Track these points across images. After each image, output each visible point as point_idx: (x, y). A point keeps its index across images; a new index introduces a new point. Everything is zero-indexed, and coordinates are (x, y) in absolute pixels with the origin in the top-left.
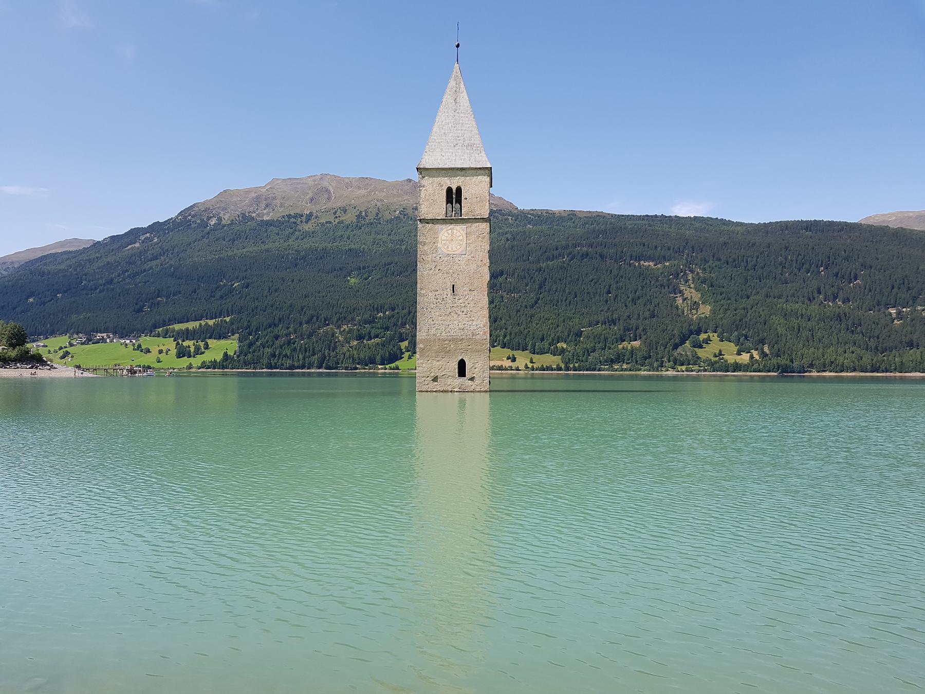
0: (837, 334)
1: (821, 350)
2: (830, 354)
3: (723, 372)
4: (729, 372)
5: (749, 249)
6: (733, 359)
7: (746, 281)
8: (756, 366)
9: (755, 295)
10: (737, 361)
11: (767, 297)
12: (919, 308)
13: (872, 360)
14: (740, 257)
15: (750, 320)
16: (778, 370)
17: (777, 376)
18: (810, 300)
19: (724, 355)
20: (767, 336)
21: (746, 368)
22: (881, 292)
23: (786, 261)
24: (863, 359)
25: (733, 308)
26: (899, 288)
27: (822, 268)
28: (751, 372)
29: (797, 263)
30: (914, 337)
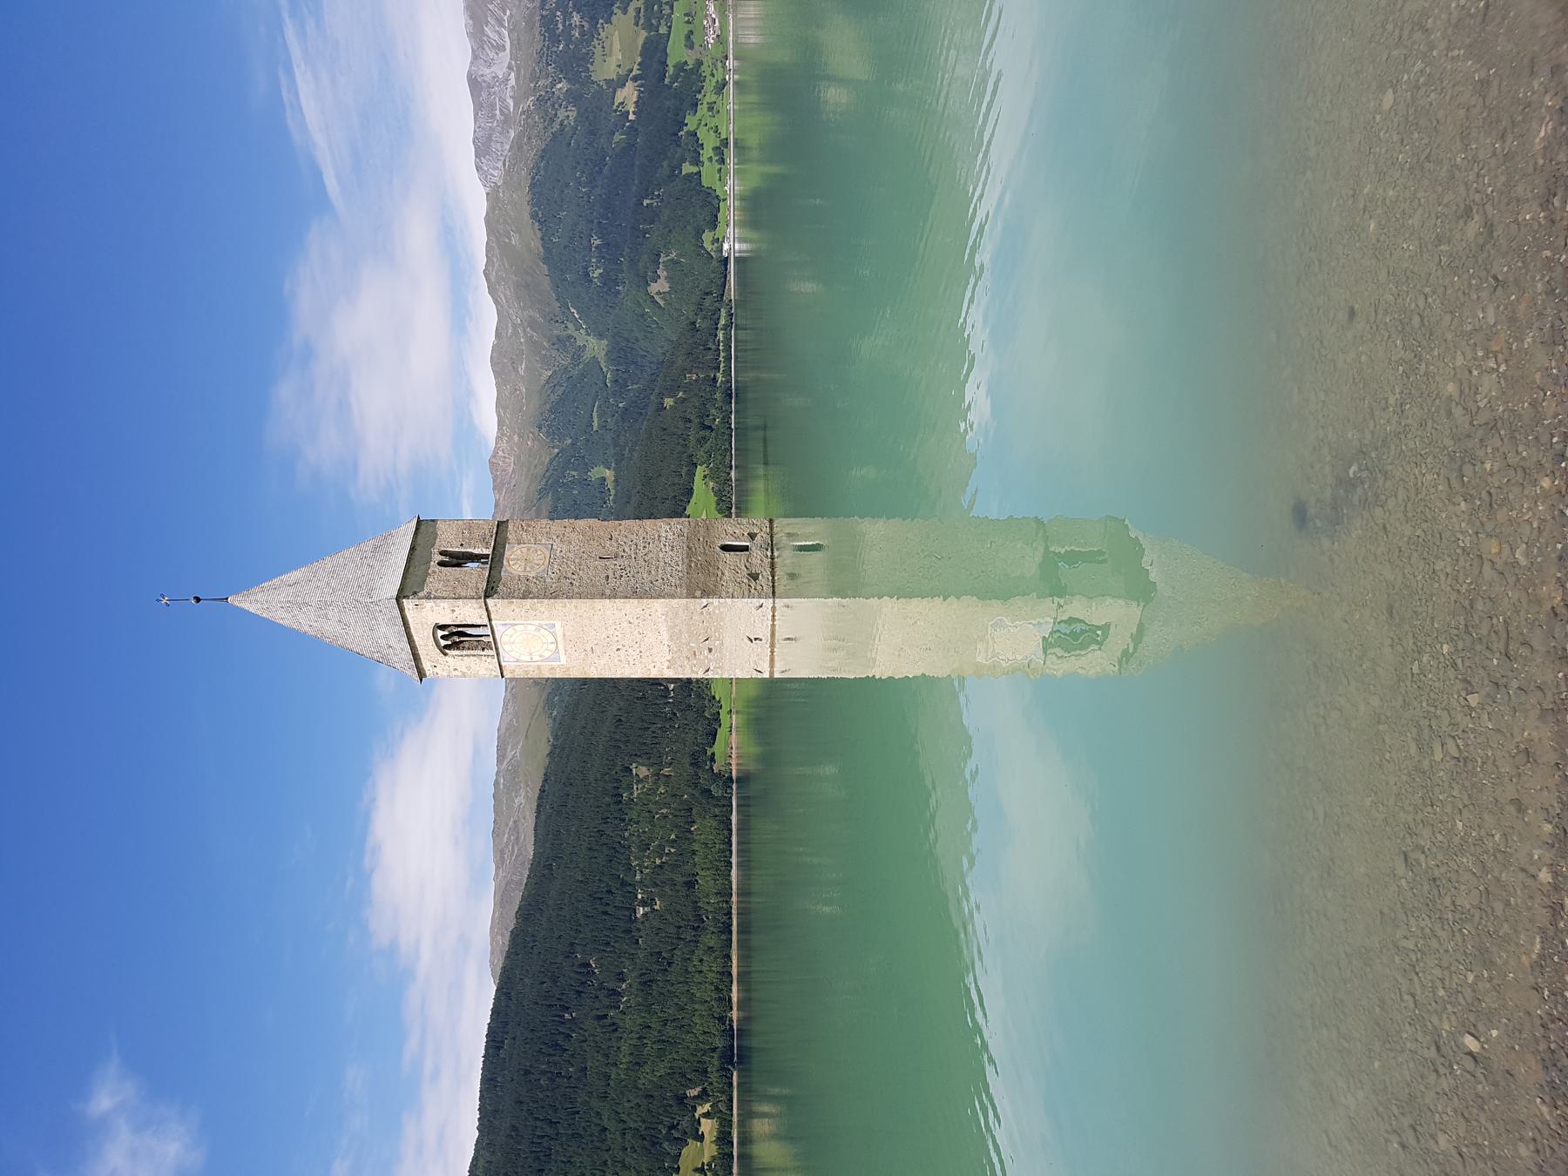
0: (673, 985)
1: (696, 1006)
2: (705, 992)
3: (732, 1163)
4: (732, 1152)
5: (522, 1137)
6: (709, 1148)
7: (576, 1136)
8: (722, 1107)
9: (601, 1118)
10: (714, 1139)
11: (606, 1097)
12: (638, 877)
13: (713, 932)
14: (534, 1149)
15: (644, 1122)
16: (729, 1070)
17: (739, 1071)
18: (616, 1030)
19: (703, 1163)
20: (671, 1091)
21: (725, 1123)
22: (612, 928)
23: (547, 1072)
24: (710, 945)
25: (620, 1153)
26: (607, 904)
27: (566, 1015)
28: (732, 1115)
29: (554, 1055)
30: (680, 879)
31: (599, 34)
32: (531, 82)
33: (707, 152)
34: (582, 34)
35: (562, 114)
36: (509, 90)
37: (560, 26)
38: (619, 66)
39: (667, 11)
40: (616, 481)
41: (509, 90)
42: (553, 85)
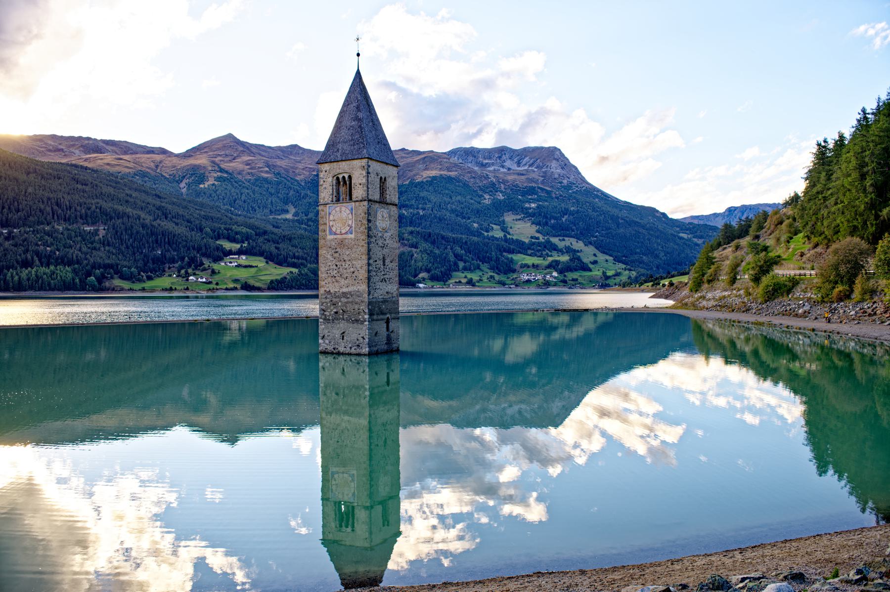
31: (526, 217)
32: (503, 180)
33: (469, 276)
34: (527, 209)
35: (487, 196)
36: (498, 168)
37: (530, 197)
38: (511, 228)
39: (538, 254)
40: (286, 219)
41: (498, 168)
42: (501, 192)
